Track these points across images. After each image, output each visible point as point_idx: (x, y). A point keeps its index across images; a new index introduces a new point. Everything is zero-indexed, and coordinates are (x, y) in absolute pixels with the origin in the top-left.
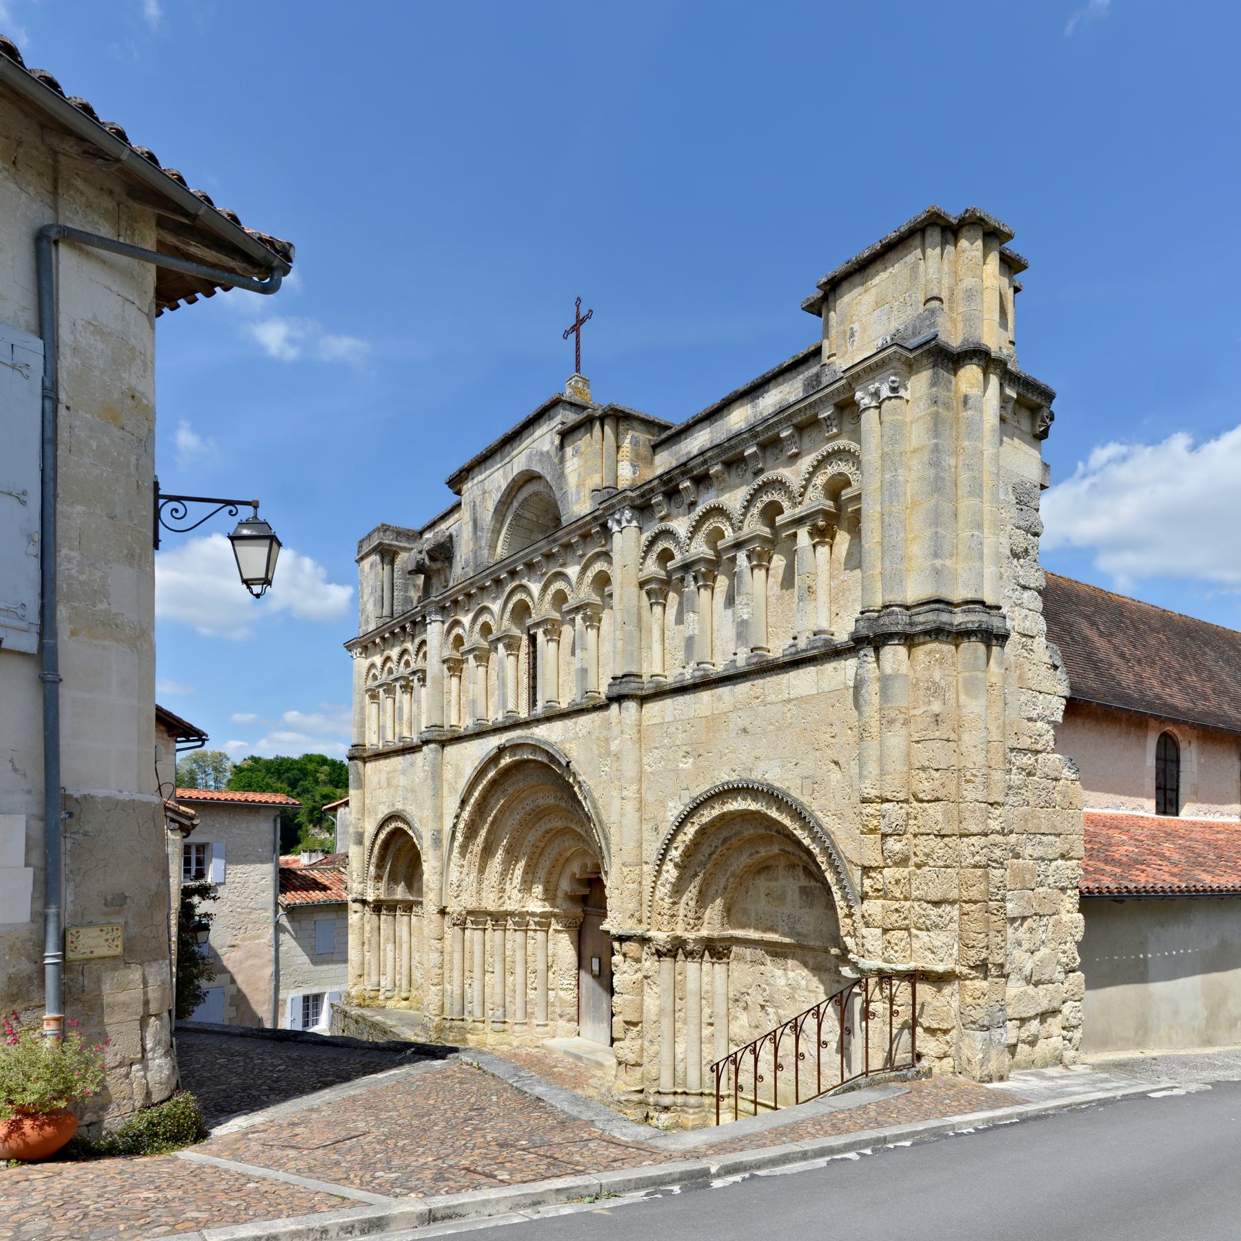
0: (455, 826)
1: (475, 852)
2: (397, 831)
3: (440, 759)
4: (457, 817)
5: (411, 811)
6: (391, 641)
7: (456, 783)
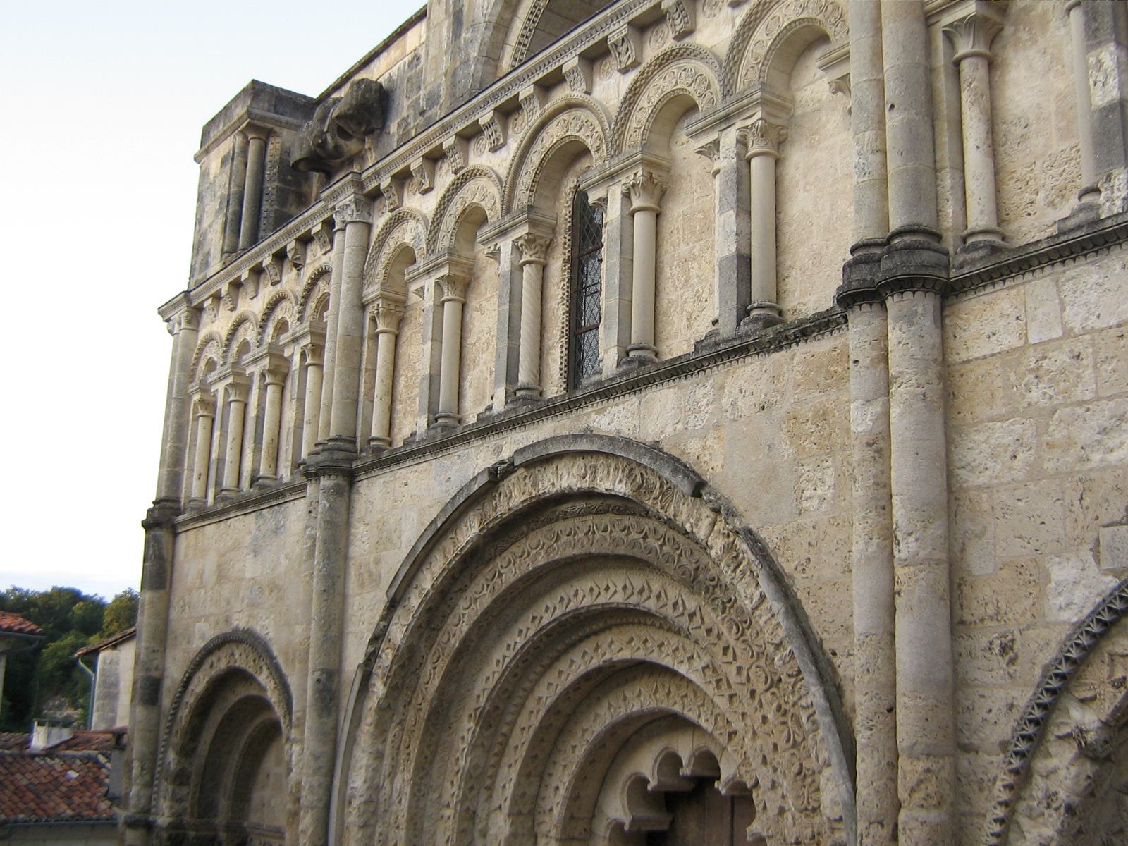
0: (371, 658)
1: (409, 723)
2: (234, 676)
3: (343, 511)
4: (378, 638)
5: (266, 626)
6: (250, 289)
7: (377, 562)
